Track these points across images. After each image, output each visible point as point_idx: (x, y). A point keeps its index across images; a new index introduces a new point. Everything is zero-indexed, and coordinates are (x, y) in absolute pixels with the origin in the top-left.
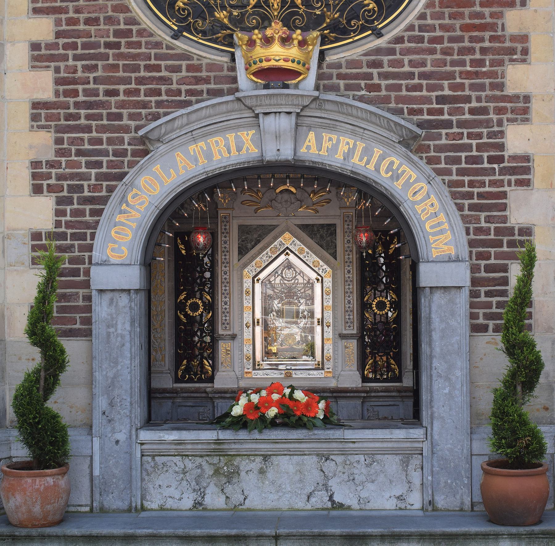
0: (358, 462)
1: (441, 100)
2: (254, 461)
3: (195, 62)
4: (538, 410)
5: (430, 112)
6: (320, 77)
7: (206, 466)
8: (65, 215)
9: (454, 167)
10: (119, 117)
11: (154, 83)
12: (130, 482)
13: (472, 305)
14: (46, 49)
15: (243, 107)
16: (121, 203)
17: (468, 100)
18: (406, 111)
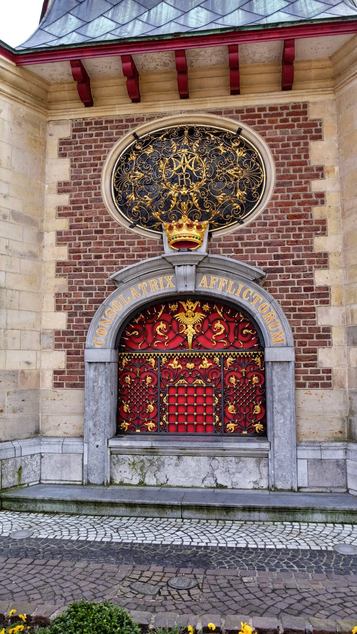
0: (231, 461)
1: (277, 257)
2: (172, 459)
3: (142, 240)
4: (336, 433)
5: (270, 264)
6: (209, 246)
7: (146, 461)
8: (73, 322)
9: (285, 294)
10: (102, 269)
12: (104, 469)
13: (296, 372)
14: (65, 235)
15: (167, 263)
16: (101, 316)
17: (292, 256)
18: (257, 264)
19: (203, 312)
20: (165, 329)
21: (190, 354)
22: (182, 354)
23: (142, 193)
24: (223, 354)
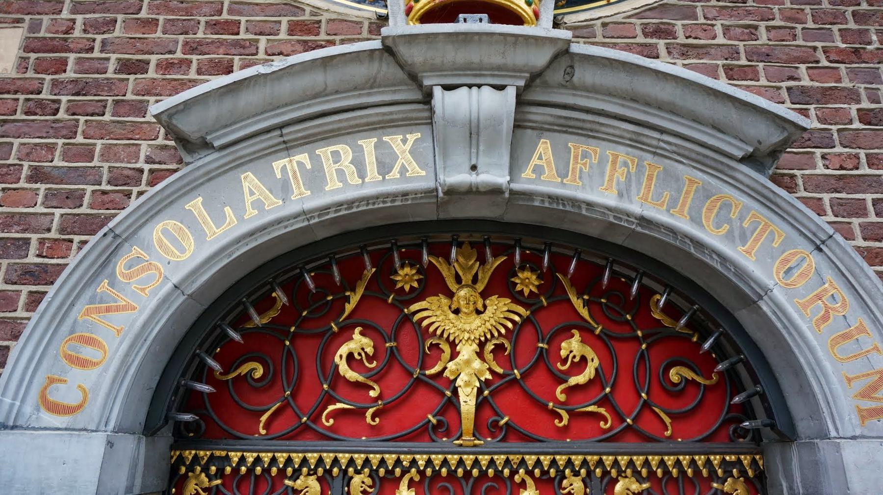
3: (306, 17)
11: (221, 51)
19: (518, 297)
20: (370, 359)
21: (469, 460)
22: (437, 459)
24: (600, 463)
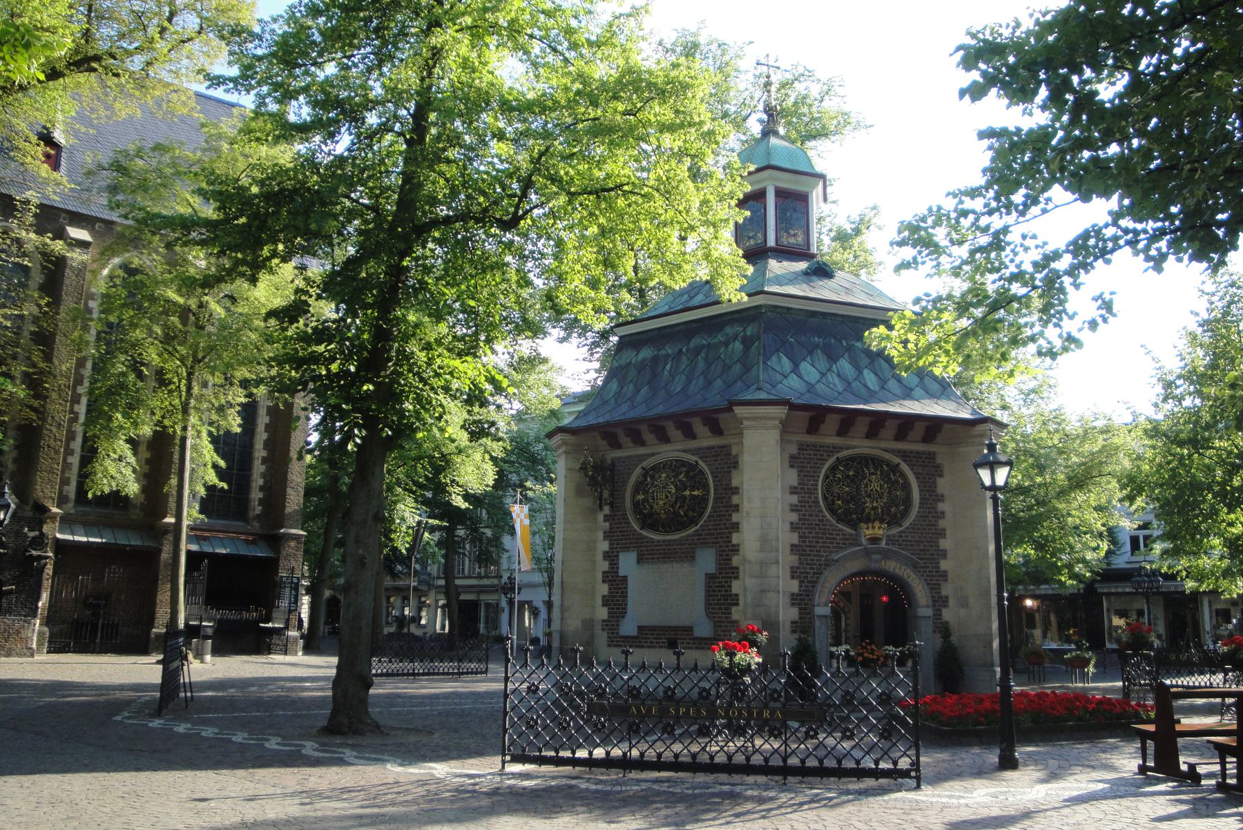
23: (848, 502)
